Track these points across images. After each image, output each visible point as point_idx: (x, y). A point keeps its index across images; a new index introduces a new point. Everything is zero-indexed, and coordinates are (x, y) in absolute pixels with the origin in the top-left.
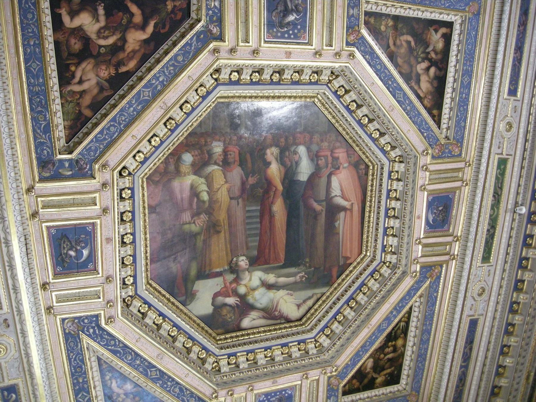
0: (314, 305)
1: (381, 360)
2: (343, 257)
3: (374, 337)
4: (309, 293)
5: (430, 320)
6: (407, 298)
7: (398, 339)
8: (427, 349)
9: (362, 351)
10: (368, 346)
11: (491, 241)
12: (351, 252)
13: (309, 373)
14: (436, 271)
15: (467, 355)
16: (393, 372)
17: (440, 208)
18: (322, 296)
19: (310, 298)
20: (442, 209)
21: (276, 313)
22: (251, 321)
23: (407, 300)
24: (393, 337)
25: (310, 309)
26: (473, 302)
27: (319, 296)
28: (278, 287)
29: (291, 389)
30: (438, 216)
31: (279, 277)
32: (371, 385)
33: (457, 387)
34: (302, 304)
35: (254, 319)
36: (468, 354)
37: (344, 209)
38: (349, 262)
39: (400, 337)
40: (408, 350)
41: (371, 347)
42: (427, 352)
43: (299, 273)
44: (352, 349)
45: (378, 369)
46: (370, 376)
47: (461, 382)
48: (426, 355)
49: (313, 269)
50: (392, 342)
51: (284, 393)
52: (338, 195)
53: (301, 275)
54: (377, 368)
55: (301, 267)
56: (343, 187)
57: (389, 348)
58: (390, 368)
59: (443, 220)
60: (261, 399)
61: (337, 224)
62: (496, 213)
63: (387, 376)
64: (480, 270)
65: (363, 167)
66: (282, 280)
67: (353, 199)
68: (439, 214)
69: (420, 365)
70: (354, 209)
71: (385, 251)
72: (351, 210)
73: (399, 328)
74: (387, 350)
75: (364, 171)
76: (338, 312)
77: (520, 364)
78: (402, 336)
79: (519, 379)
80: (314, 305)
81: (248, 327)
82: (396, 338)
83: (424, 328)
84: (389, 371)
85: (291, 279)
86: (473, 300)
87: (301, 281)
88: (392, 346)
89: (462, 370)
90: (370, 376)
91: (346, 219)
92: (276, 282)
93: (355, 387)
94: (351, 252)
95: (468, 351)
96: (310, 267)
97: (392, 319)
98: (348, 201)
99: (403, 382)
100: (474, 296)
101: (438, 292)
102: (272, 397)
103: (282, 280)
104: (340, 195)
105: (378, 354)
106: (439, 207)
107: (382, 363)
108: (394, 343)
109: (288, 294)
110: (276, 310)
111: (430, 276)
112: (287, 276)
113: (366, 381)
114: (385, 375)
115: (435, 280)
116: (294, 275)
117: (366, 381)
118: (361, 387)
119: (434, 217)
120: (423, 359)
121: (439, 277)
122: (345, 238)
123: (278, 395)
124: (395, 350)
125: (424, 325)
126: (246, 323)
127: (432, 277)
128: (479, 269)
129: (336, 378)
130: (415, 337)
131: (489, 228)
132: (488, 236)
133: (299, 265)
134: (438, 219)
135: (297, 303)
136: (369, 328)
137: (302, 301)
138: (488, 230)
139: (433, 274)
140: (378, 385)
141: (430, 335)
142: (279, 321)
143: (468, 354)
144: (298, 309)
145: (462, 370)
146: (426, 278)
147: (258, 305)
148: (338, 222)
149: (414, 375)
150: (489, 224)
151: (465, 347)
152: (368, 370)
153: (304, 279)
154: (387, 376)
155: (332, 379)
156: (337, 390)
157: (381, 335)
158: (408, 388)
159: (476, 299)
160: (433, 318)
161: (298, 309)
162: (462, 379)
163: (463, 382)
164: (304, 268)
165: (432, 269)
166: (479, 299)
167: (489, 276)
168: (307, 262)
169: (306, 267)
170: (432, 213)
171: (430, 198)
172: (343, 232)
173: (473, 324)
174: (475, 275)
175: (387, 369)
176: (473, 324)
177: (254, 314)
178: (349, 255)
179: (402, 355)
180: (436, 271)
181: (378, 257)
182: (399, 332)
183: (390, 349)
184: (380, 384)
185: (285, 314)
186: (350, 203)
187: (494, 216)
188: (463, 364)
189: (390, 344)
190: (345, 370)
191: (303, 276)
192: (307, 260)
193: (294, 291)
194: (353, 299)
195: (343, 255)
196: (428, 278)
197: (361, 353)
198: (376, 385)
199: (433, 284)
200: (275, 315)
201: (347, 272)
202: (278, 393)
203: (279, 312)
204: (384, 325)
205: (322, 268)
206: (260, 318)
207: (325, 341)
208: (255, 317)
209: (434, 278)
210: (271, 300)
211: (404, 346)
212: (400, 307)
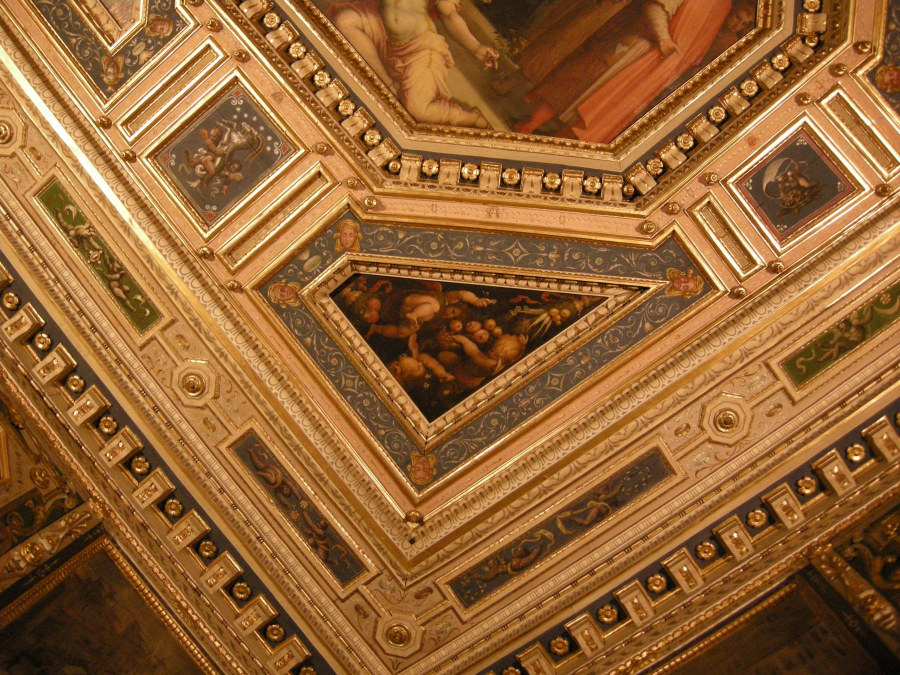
0: (460, 125)
1: (449, 330)
2: (576, 110)
3: (480, 249)
4: (473, 97)
5: (592, 362)
6: (599, 261)
7: (511, 334)
8: (536, 410)
9: (439, 244)
10: (457, 251)
11: (834, 351)
12: (597, 119)
13: (332, 154)
14: (691, 285)
15: (584, 515)
16: (446, 384)
17: (803, 182)
18: (486, 128)
19: (465, 107)
20: (805, 189)
21: (400, 64)
22: (357, 28)
23: (595, 266)
24: (508, 318)
25: (448, 124)
26: (694, 425)
27: (481, 122)
28: (444, 26)
29: (284, 149)
30: (786, 191)
31: (462, 13)
32: (389, 351)
33: (504, 553)
34: (445, 100)
35: (363, 31)
36: (589, 519)
37: (654, 41)
38: (576, 130)
39: (518, 335)
40: (505, 377)
41: (458, 259)
42: (530, 414)
43: (495, 48)
44: (430, 214)
45: (430, 341)
46: (405, 331)
47: (521, 557)
48: (522, 419)
49: (517, 67)
50: (497, 325)
51: (269, 138)
52: (667, 8)
53: (492, 52)
54: (431, 335)
55: (505, 42)
56: (688, 6)
57: (483, 328)
58: (447, 370)
59: (787, 211)
60: (234, 103)
61: (620, 49)
62: (890, 311)
63: (427, 376)
64: (763, 378)
65: (746, 18)
66: (459, 24)
67: (683, 44)
68: (793, 189)
69: (494, 422)
70: (667, 61)
71: (646, 164)
72: (663, 57)
73: (533, 317)
74: (475, 326)
75: (740, 27)
76: (478, 162)
77: (653, 631)
78: (524, 340)
79: (619, 657)
80: (460, 125)
81: (344, 31)
82: (510, 329)
83: (570, 361)
84: (440, 371)
85: (472, 41)
86: (697, 416)
87: (482, 63)
88: (491, 332)
89: (548, 534)
90: (405, 331)
91: (641, 61)
92: (449, 17)
93: (366, 315)
94: (597, 119)
95: (593, 512)
96: (516, 59)
97: (539, 262)
98: (672, 37)
99: (439, 422)
100: (708, 410)
101: (656, 326)
102: (249, 121)
103: (459, 24)
104: (671, 14)
105: (458, 311)
106: (802, 176)
107: (445, 337)
108: (498, 330)
109: (444, 57)
110: (403, 58)
111: (672, 280)
112: (474, 29)
113: (391, 330)
114: (428, 370)
115: (672, 299)
116: (484, 41)
117: (391, 330)
118: (373, 326)
119: (776, 183)
120: (511, 419)
121: (684, 303)
122: (609, 85)
123: (259, 132)
124: (487, 347)
125: (575, 353)
126: (350, 20)
127: (673, 288)
128: (765, 371)
129: (356, 231)
130: (540, 362)
131: (855, 322)
132: (838, 334)
133: (504, 36)
134: (782, 194)
135: (441, 91)
136: (490, 215)
137: (450, 97)
138: (847, 322)
139: (680, 283)
140: (398, 368)
141: (566, 389)
142: (389, 81)
143: (589, 519)
144: (433, 101)
145: (548, 534)
146: (660, 271)
147: (391, 17)
148: (625, 49)
149: (464, 427)
150: (860, 313)
151: (594, 494)
152: (413, 316)
153: (490, 65)
154: (427, 376)
155: (350, 222)
156: (337, 255)
157: (495, 262)
158: (433, 439)
159: (705, 424)
160: (601, 364)
161: (433, 101)
162: (526, 553)
163: (524, 561)
164: (508, 49)
165: (685, 270)
166: (710, 432)
167: (770, 415)
168: (520, 46)
169: (512, 50)
170: (780, 170)
171: (802, 141)
172: (616, 74)
173: (652, 469)
174: (746, 375)
175: (442, 363)
176: (652, 469)
177: (371, 22)
178: (588, 120)
179: (489, 375)
180: (691, 285)
181: (626, 158)
182: (526, 324)
183: (481, 332)
184: (402, 373)
185: (408, 83)
186: (672, 44)
187: (882, 311)
188: (560, 525)
189: (491, 322)
190: (382, 238)
191: (491, 59)
192: (524, 43)
193: (456, 64)
194: (520, 172)
195: (580, 109)
196: (665, 278)
197: (434, 245)
198: (394, 365)
199: (662, 300)
200: (395, 63)
201: (558, 140)
202: (262, 128)
203: (405, 68)
204: (517, 252)
205: (530, 86)
206: (373, 41)
207: (410, 168)
208: (368, 29)
209: (676, 293)
210: (414, 33)
211: (508, 363)
212: (570, 257)
